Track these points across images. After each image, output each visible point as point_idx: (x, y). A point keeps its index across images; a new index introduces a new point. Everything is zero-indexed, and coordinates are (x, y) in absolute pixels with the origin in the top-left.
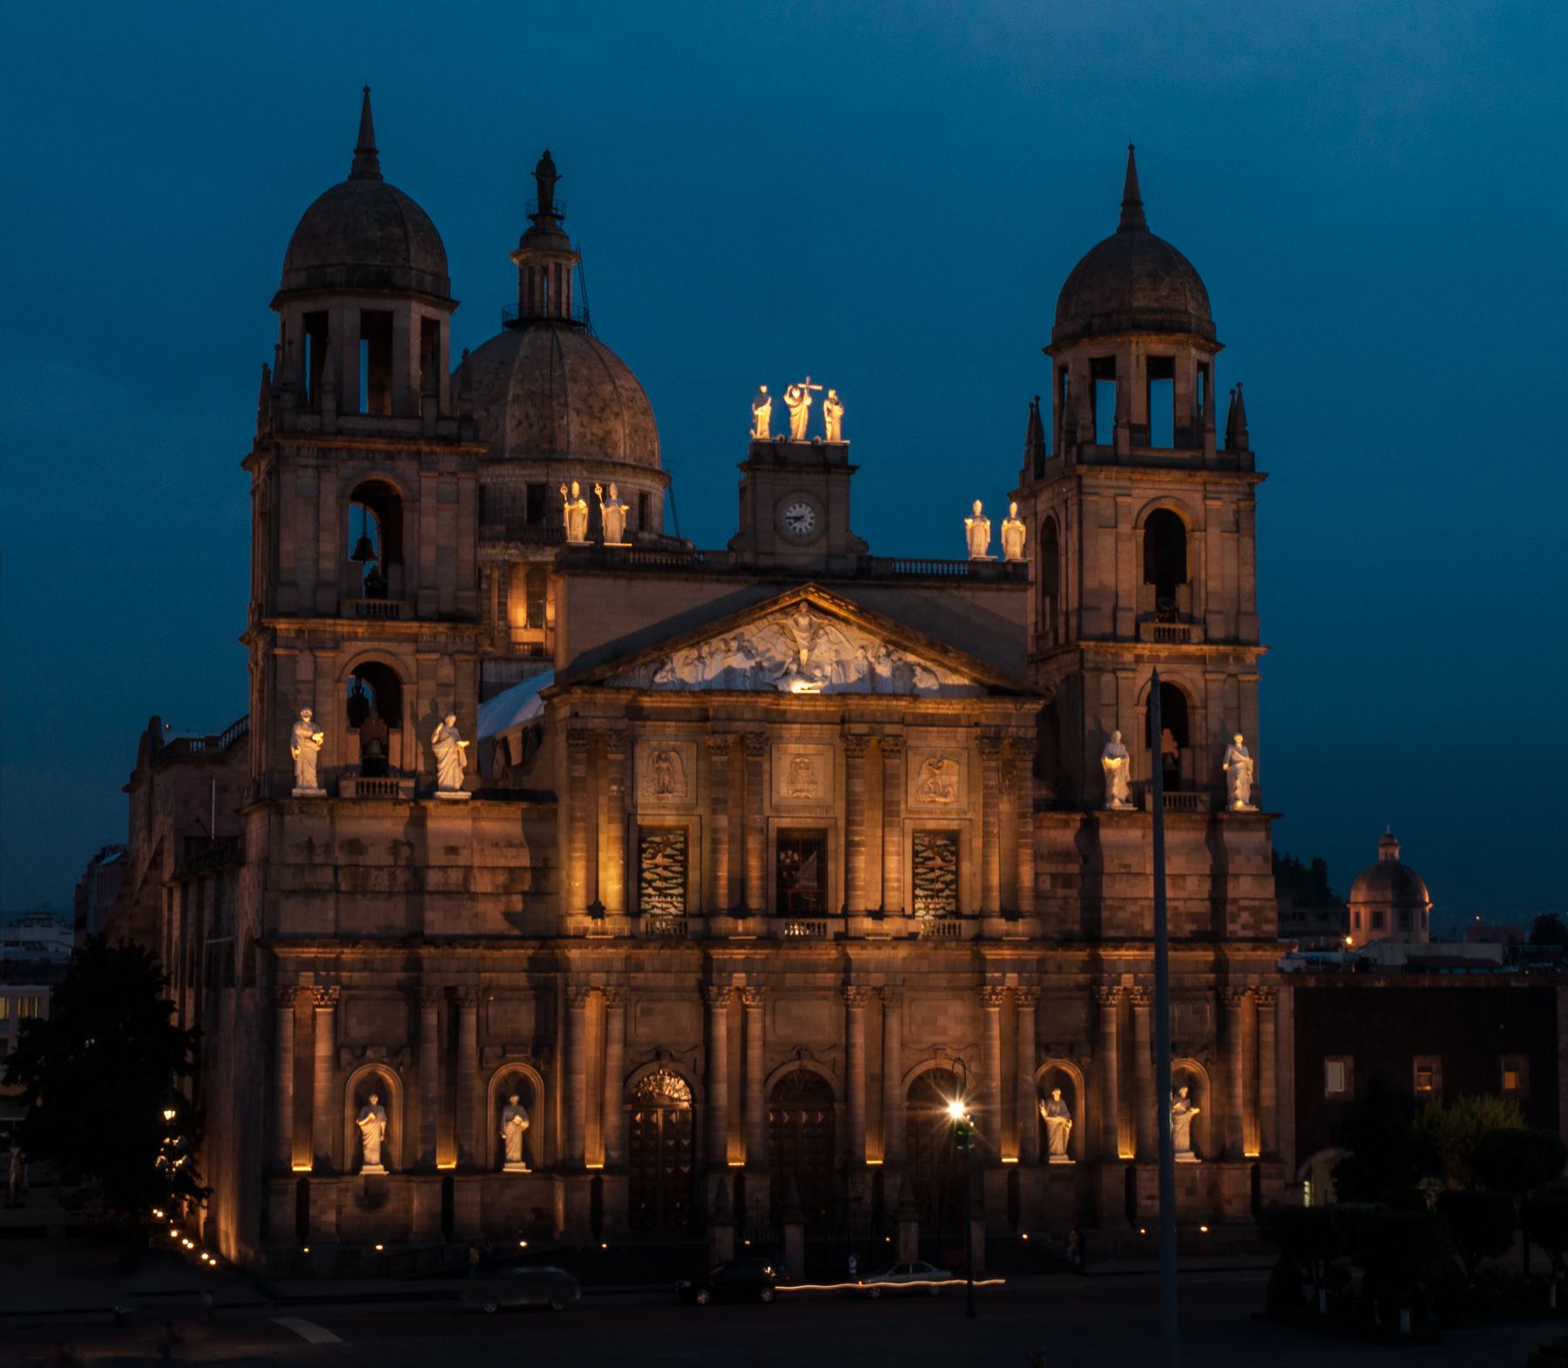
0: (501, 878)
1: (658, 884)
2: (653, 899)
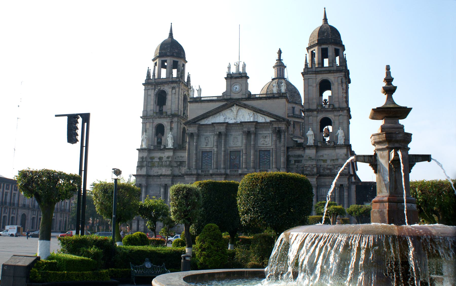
1: (206, 163)
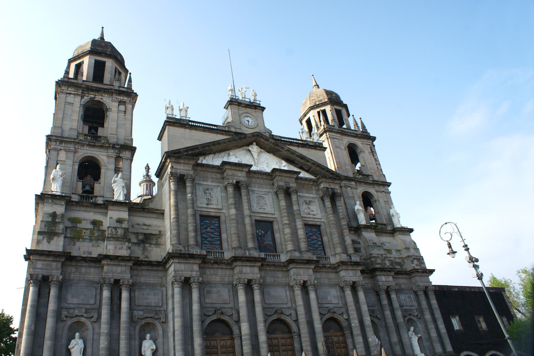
1: (209, 239)
2: (208, 245)
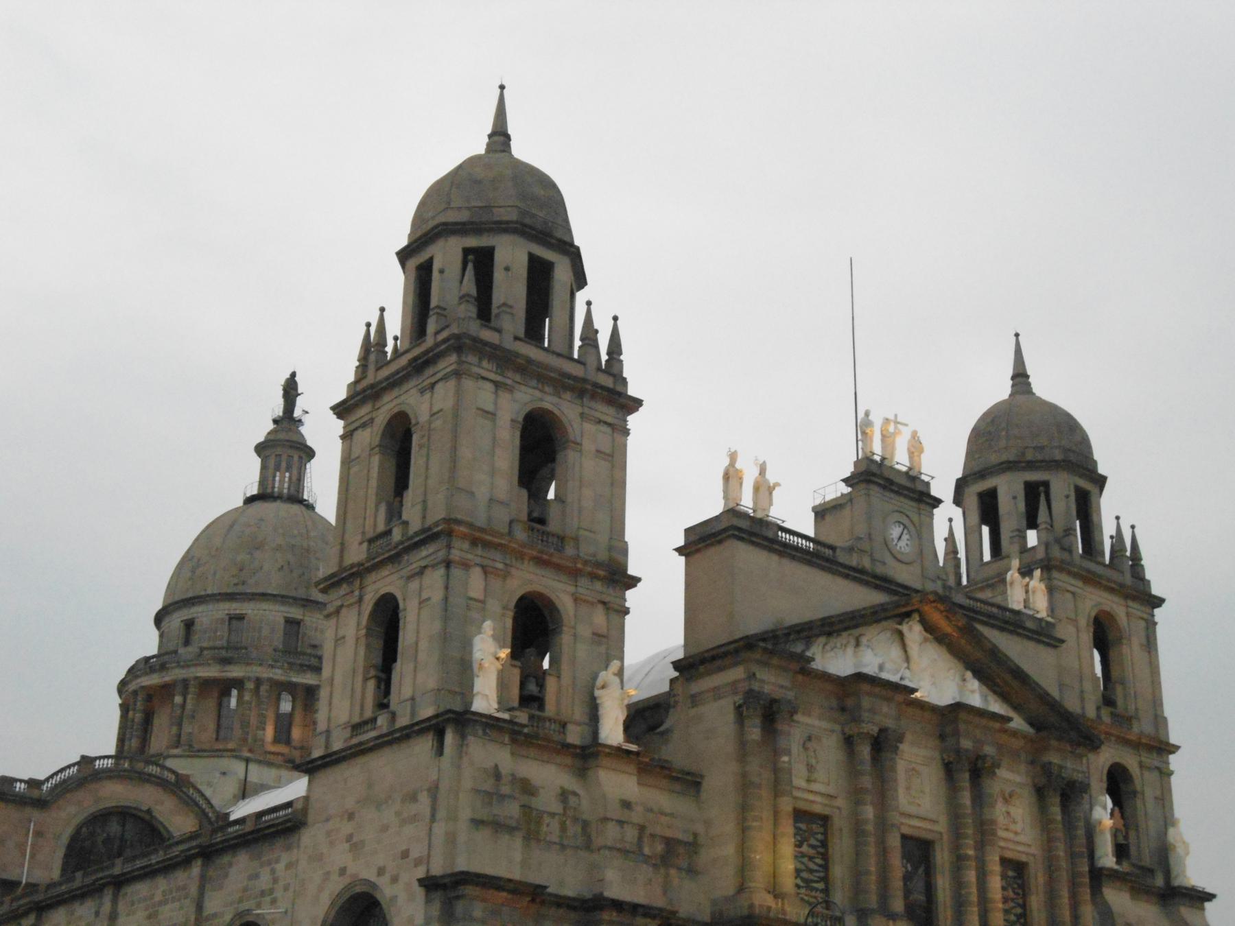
0: (660, 848)
